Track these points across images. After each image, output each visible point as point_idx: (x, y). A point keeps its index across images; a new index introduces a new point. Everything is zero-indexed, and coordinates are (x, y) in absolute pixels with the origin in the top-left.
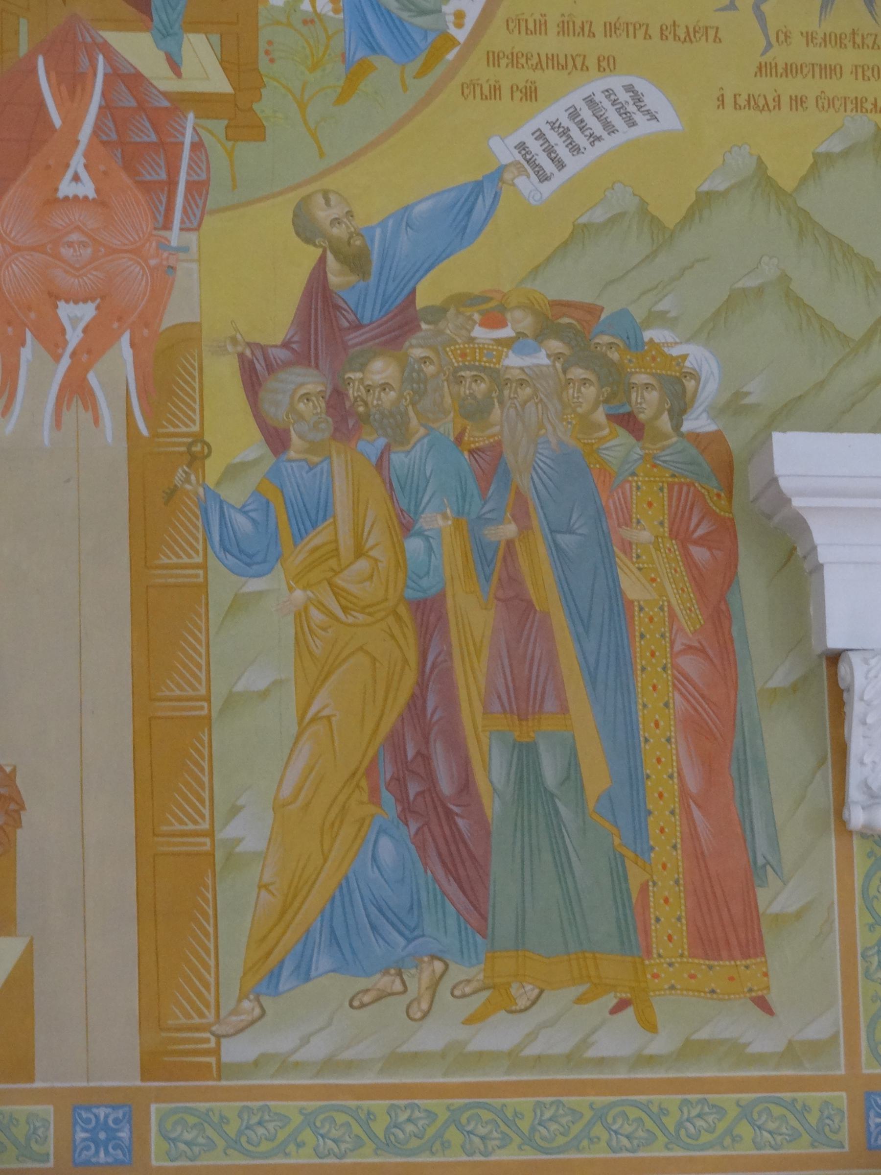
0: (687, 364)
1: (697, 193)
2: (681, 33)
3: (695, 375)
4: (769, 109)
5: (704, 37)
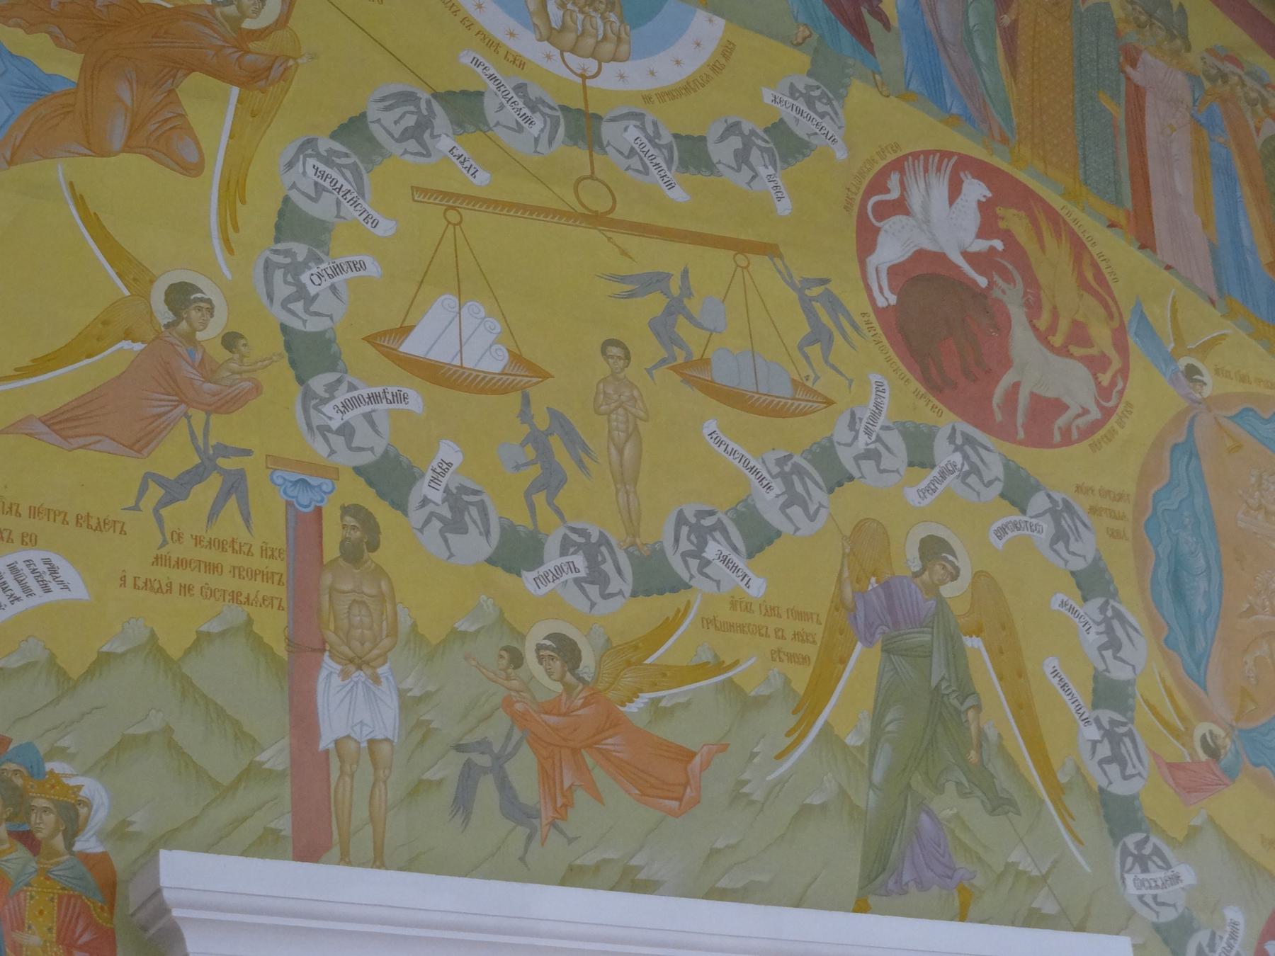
0: (82, 793)
1: (99, 653)
2: (94, 522)
3: (87, 803)
4: (162, 592)
5: (112, 528)
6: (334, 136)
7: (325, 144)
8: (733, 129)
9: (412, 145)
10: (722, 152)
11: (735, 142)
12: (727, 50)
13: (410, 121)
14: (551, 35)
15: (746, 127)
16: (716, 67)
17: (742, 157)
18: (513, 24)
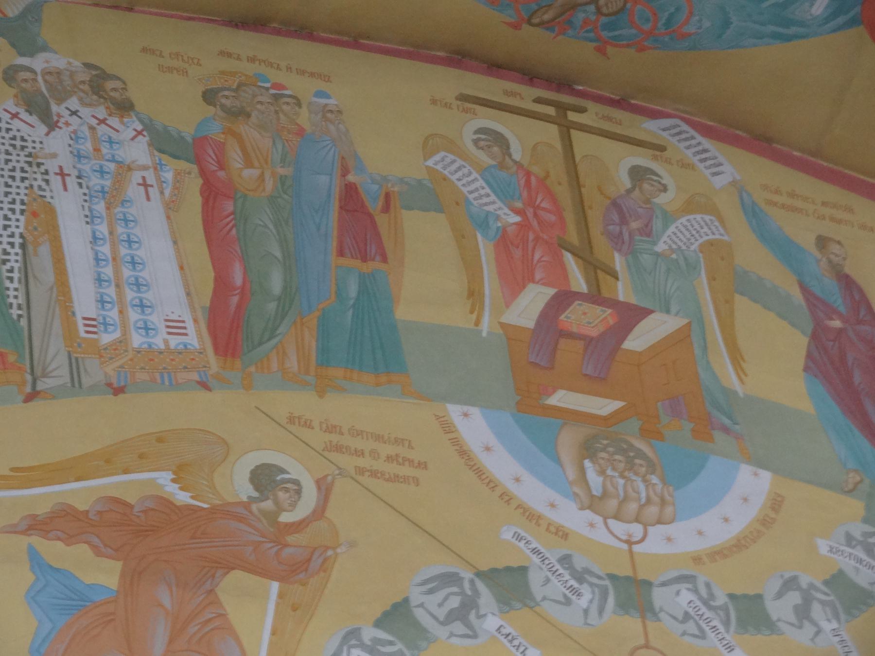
6: (378, 624)
7: (369, 633)
8: (790, 584)
9: (458, 627)
11: (794, 598)
12: (776, 503)
13: (455, 602)
14: (593, 503)
15: (805, 580)
16: (765, 522)
17: (803, 613)
18: (551, 494)
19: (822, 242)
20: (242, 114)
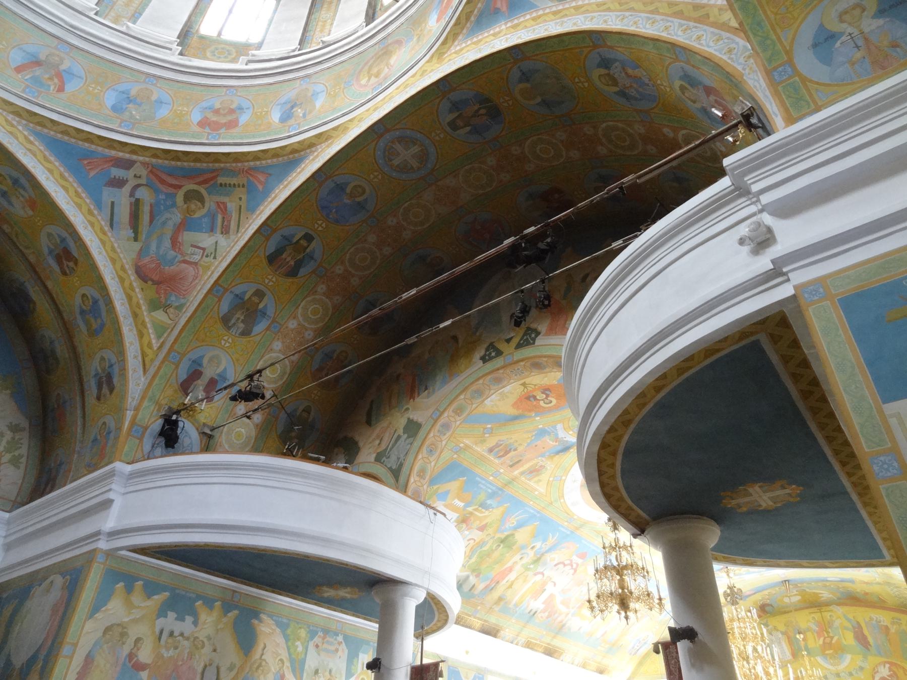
10: (854, 673)
17: (856, 672)
19: (854, 617)
20: (788, 626)
